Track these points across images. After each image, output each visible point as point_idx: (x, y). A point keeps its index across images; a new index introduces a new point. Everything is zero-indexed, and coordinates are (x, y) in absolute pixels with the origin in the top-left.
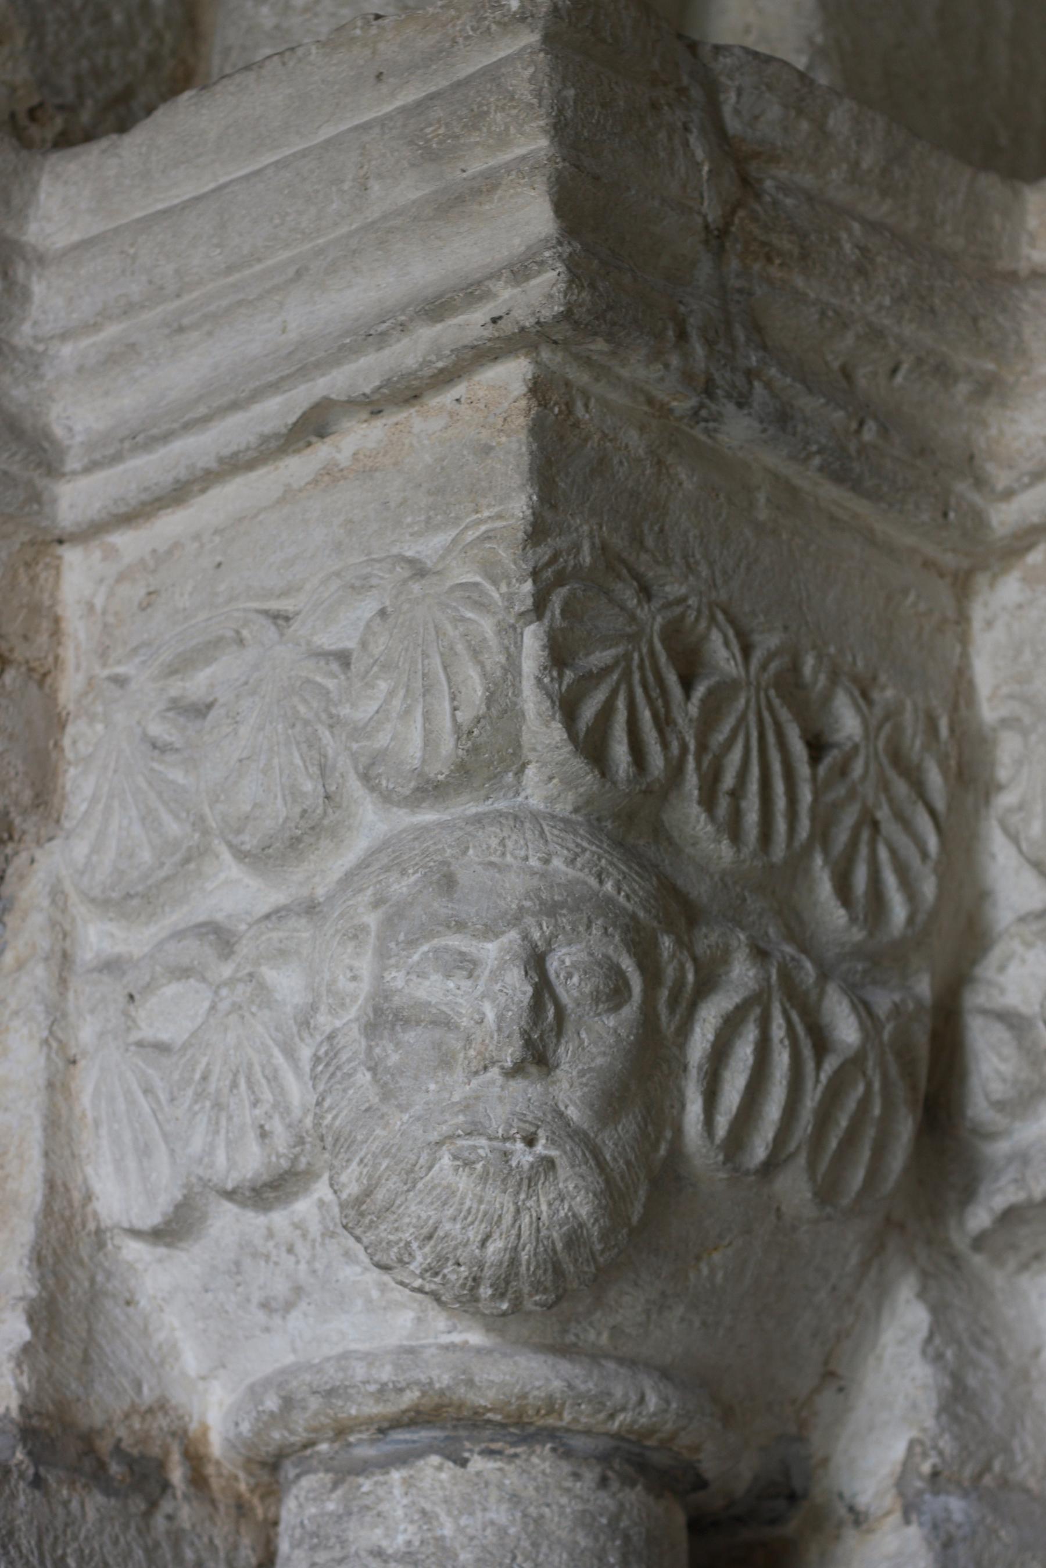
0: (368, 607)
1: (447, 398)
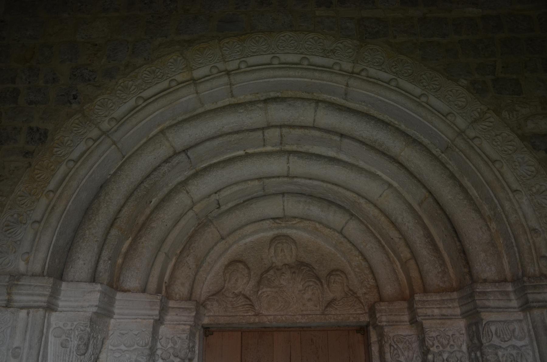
0: (138, 332)
1: (147, 320)
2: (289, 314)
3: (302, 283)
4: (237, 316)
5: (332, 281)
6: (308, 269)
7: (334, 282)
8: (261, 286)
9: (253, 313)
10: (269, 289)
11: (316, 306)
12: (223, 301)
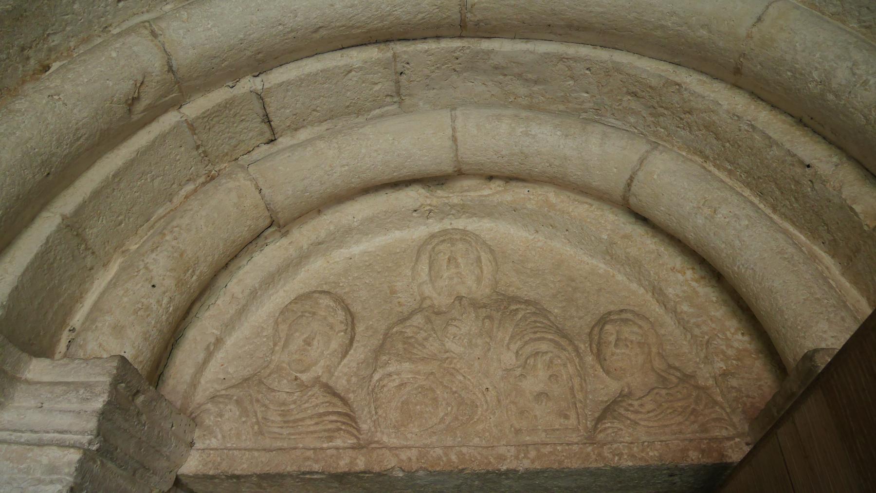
2: (471, 444)
3: (514, 347)
4: (295, 448)
5: (612, 338)
6: (531, 309)
7: (618, 340)
8: (384, 358)
9: (351, 441)
10: (407, 365)
11: (566, 417)
12: (258, 401)
